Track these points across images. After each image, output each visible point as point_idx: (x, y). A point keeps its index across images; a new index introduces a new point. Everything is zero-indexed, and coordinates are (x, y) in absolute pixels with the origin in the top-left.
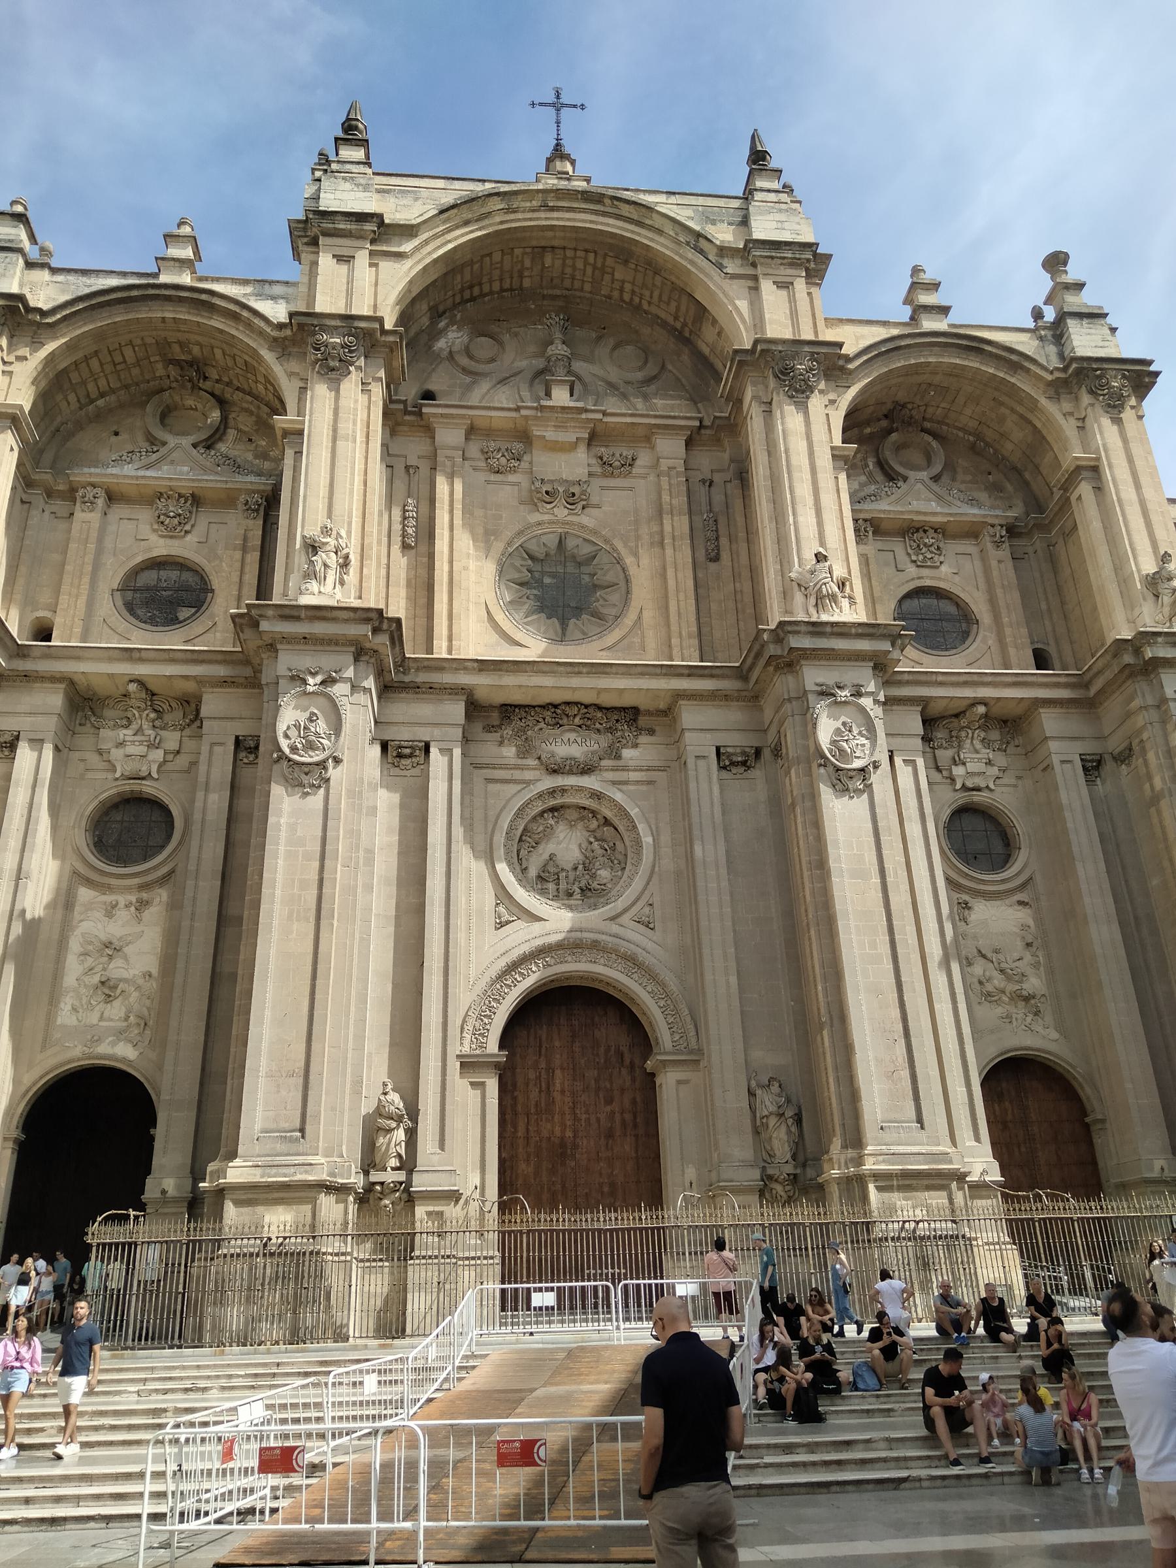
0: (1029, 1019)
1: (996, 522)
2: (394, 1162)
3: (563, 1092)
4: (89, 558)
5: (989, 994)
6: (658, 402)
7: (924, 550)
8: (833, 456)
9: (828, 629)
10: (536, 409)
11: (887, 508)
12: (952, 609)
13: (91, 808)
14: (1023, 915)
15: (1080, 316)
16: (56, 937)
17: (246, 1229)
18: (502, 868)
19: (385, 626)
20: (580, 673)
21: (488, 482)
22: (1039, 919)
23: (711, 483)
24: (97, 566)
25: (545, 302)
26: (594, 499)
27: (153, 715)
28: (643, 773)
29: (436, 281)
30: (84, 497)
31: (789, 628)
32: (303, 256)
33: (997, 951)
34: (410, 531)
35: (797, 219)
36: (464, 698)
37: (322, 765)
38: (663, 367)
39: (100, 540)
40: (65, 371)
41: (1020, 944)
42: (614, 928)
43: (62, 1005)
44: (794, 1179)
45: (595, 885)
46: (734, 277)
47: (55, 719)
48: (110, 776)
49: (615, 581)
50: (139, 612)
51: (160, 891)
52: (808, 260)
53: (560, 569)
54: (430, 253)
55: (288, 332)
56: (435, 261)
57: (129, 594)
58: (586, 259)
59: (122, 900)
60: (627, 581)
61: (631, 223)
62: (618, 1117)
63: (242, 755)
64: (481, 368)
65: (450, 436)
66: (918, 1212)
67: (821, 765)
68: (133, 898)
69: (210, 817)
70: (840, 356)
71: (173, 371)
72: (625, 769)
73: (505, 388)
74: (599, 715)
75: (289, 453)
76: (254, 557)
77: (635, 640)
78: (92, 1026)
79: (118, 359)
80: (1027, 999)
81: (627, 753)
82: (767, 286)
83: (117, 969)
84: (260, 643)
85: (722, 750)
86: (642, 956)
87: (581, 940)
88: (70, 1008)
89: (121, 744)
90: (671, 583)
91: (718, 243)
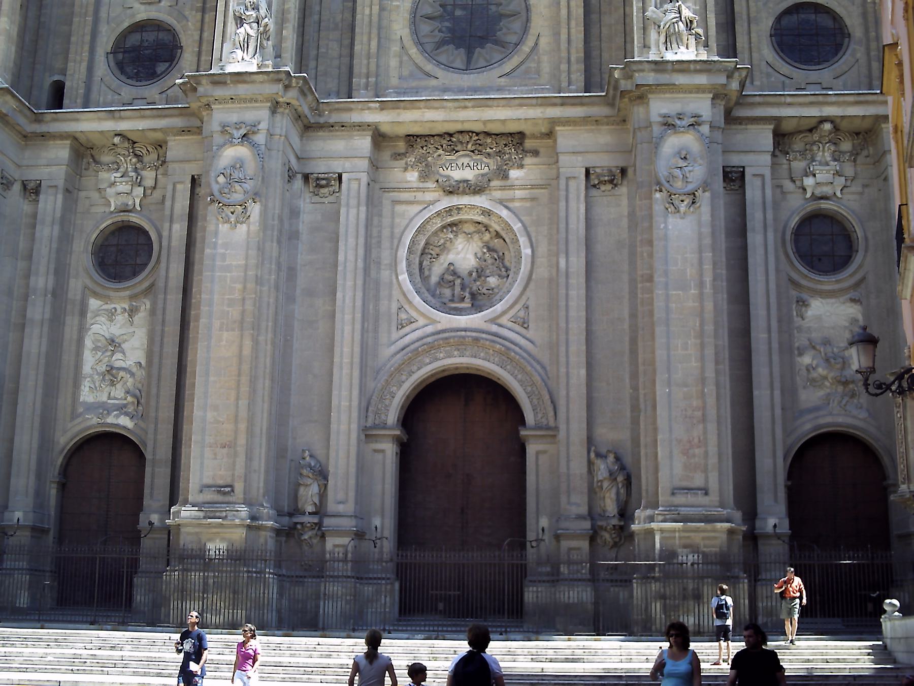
0: (844, 402)
2: (310, 508)
4: (88, 29)
5: (813, 381)
12: (830, 23)
13: (95, 236)
16: (75, 337)
17: (194, 553)
18: (404, 277)
19: (294, 85)
20: (466, 107)
24: (94, 34)
27: (134, 160)
28: (527, 191)
36: (370, 133)
43: (82, 387)
47: (64, 167)
50: (128, 69)
51: (145, 300)
57: (120, 56)
60: (528, 9)
66: (690, 557)
69: (174, 243)
72: (511, 187)
74: (489, 140)
77: (533, 65)
78: (104, 403)
81: (514, 174)
83: (118, 360)
84: (200, 104)
88: (87, 389)
89: (113, 184)
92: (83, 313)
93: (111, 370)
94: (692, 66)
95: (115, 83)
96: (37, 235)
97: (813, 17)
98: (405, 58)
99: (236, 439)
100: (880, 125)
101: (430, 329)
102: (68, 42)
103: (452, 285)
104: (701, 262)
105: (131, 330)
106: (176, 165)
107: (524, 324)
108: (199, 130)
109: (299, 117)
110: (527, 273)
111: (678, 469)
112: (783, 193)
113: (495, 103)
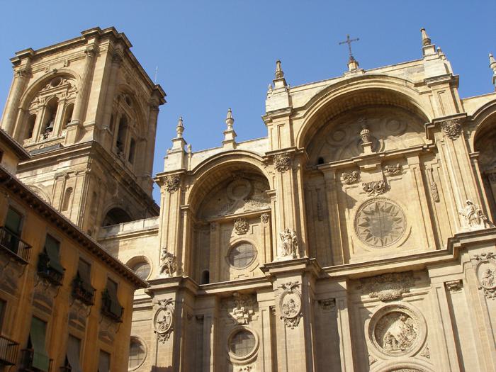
8: (471, 158)
21: (347, 188)
23: (432, 170)
24: (220, 249)
29: (316, 121)
34: (320, 215)
37: (295, 318)
38: (407, 126)
39: (220, 241)
42: (413, 360)
46: (422, 93)
49: (400, 217)
59: (243, 367)
64: (341, 143)
68: (246, 367)
70: (467, 117)
74: (397, 276)
76: (268, 237)
82: (434, 94)
96: (204, 338)
101: (384, 364)
102: (209, 254)
103: (391, 343)
107: (428, 356)
108: (271, 287)
109: (314, 276)
110: (425, 332)
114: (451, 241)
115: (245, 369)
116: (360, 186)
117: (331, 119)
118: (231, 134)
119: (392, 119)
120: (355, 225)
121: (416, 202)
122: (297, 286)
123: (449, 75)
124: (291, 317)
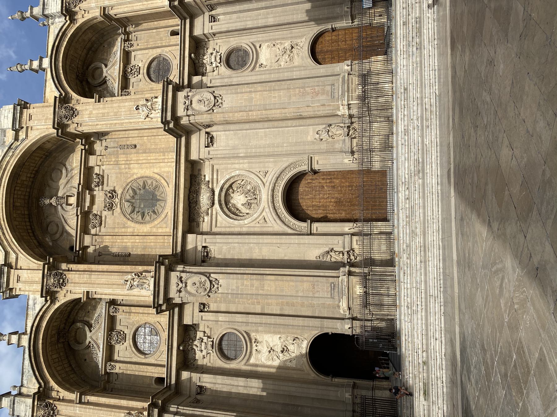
0: (299, 48)
1: (123, 45)
3: (320, 202)
6: (74, 165)
7: (133, 71)
8: (99, 101)
9: (164, 106)
10: (77, 209)
11: (117, 84)
12: (155, 63)
14: (264, 46)
15: (44, 9)
17: (361, 300)
21: (105, 227)
22: (266, 41)
25: (34, 206)
26: (113, 189)
27: (191, 341)
30: (110, 370)
31: (164, 120)
32: (17, 294)
33: (276, 56)
35: (3, 111)
40: (62, 378)
41: (274, 48)
42: (267, 184)
43: (289, 366)
44: (348, 127)
45: (252, 191)
47: (192, 374)
48: (212, 354)
49: (142, 181)
52: (20, 108)
53: (138, 201)
54: (16, 247)
55: (48, 298)
56: (19, 245)
58: (18, 190)
59: (254, 348)
61: (4, 173)
62: (328, 184)
63: (206, 310)
65: (87, 240)
67: (213, 112)
68: (254, 345)
70: (60, 98)
71: (61, 340)
73: (68, 221)
74: (193, 188)
75: (95, 296)
77: (165, 175)
79: (57, 360)
80: (292, 47)
81: (207, 179)
82: (30, 124)
83: (279, 349)
85: (206, 145)
86: (276, 175)
87: (271, 195)
88: (290, 363)
89: (202, 351)
90: (144, 161)
91: (13, 141)
92: (256, 365)
93: (282, 352)
94: (165, 98)
95: (158, 353)
97: (152, 69)
98: (159, 226)
99: (310, 282)
100: (193, 36)
101: (267, 210)
104: (242, 93)
105: (265, 342)
106: (194, 319)
110: (246, 172)
111: (324, 97)
112: (218, 75)
113: (177, 182)
114: (167, 128)
115: (257, 346)
116: (104, 213)
117: (33, 232)
118: (13, 336)
119: (51, 175)
120: (142, 223)
121: (132, 166)
122: (181, 278)
123: (14, 107)
124: (209, 286)
